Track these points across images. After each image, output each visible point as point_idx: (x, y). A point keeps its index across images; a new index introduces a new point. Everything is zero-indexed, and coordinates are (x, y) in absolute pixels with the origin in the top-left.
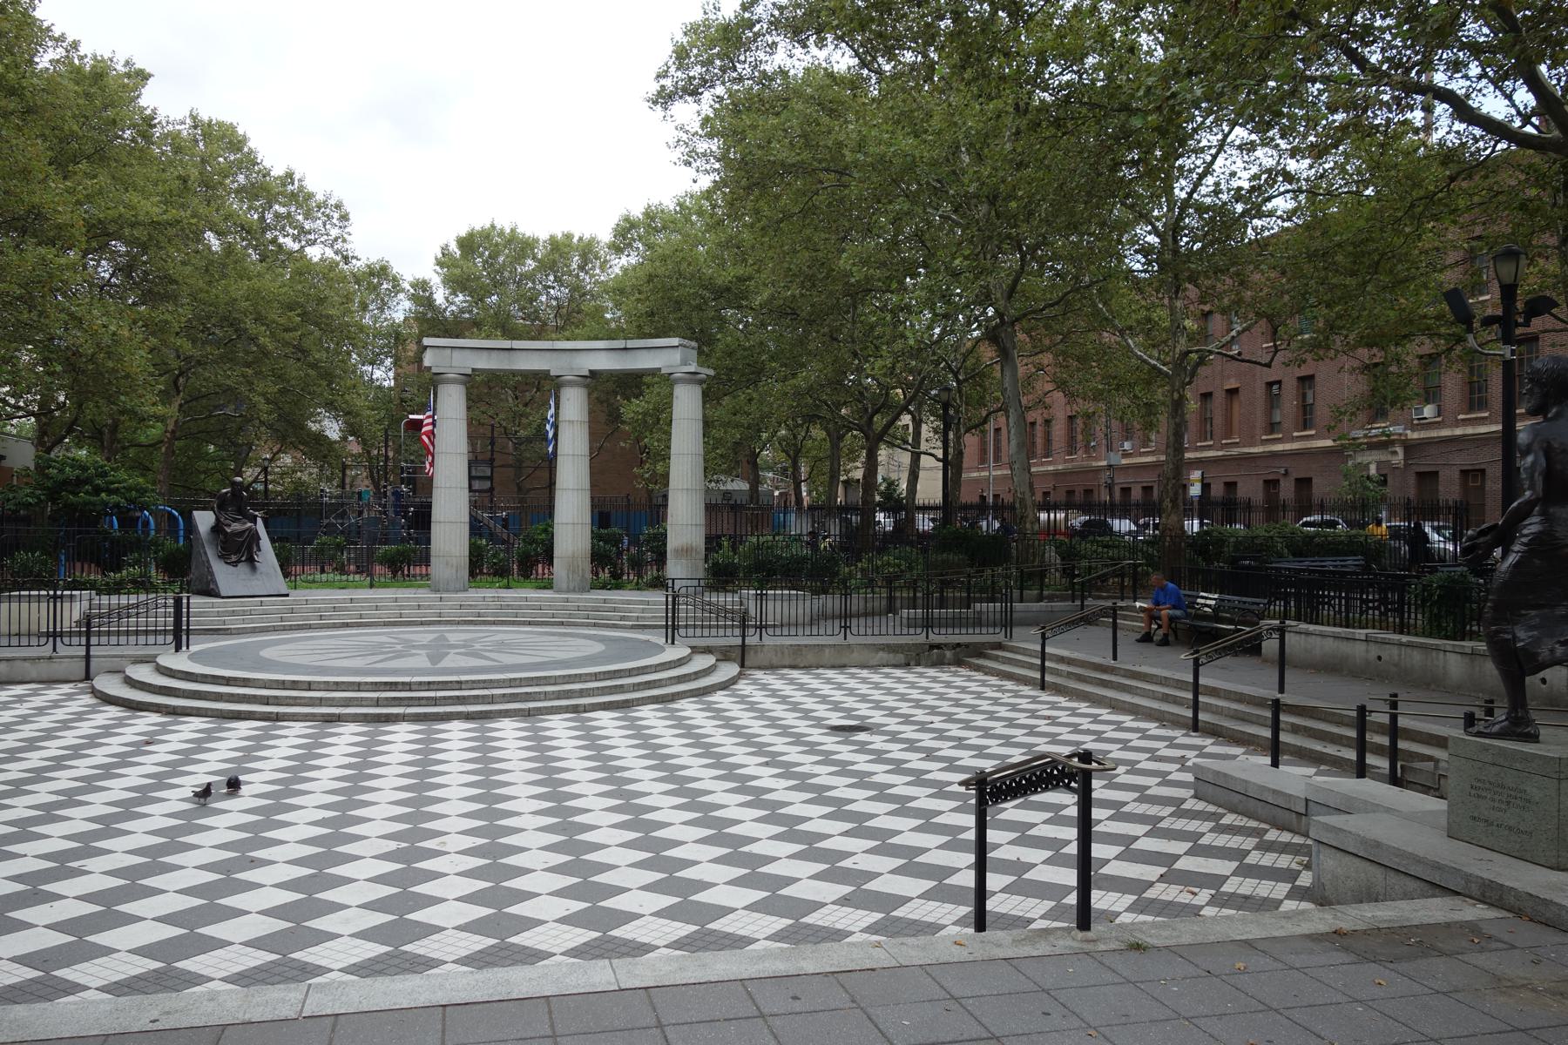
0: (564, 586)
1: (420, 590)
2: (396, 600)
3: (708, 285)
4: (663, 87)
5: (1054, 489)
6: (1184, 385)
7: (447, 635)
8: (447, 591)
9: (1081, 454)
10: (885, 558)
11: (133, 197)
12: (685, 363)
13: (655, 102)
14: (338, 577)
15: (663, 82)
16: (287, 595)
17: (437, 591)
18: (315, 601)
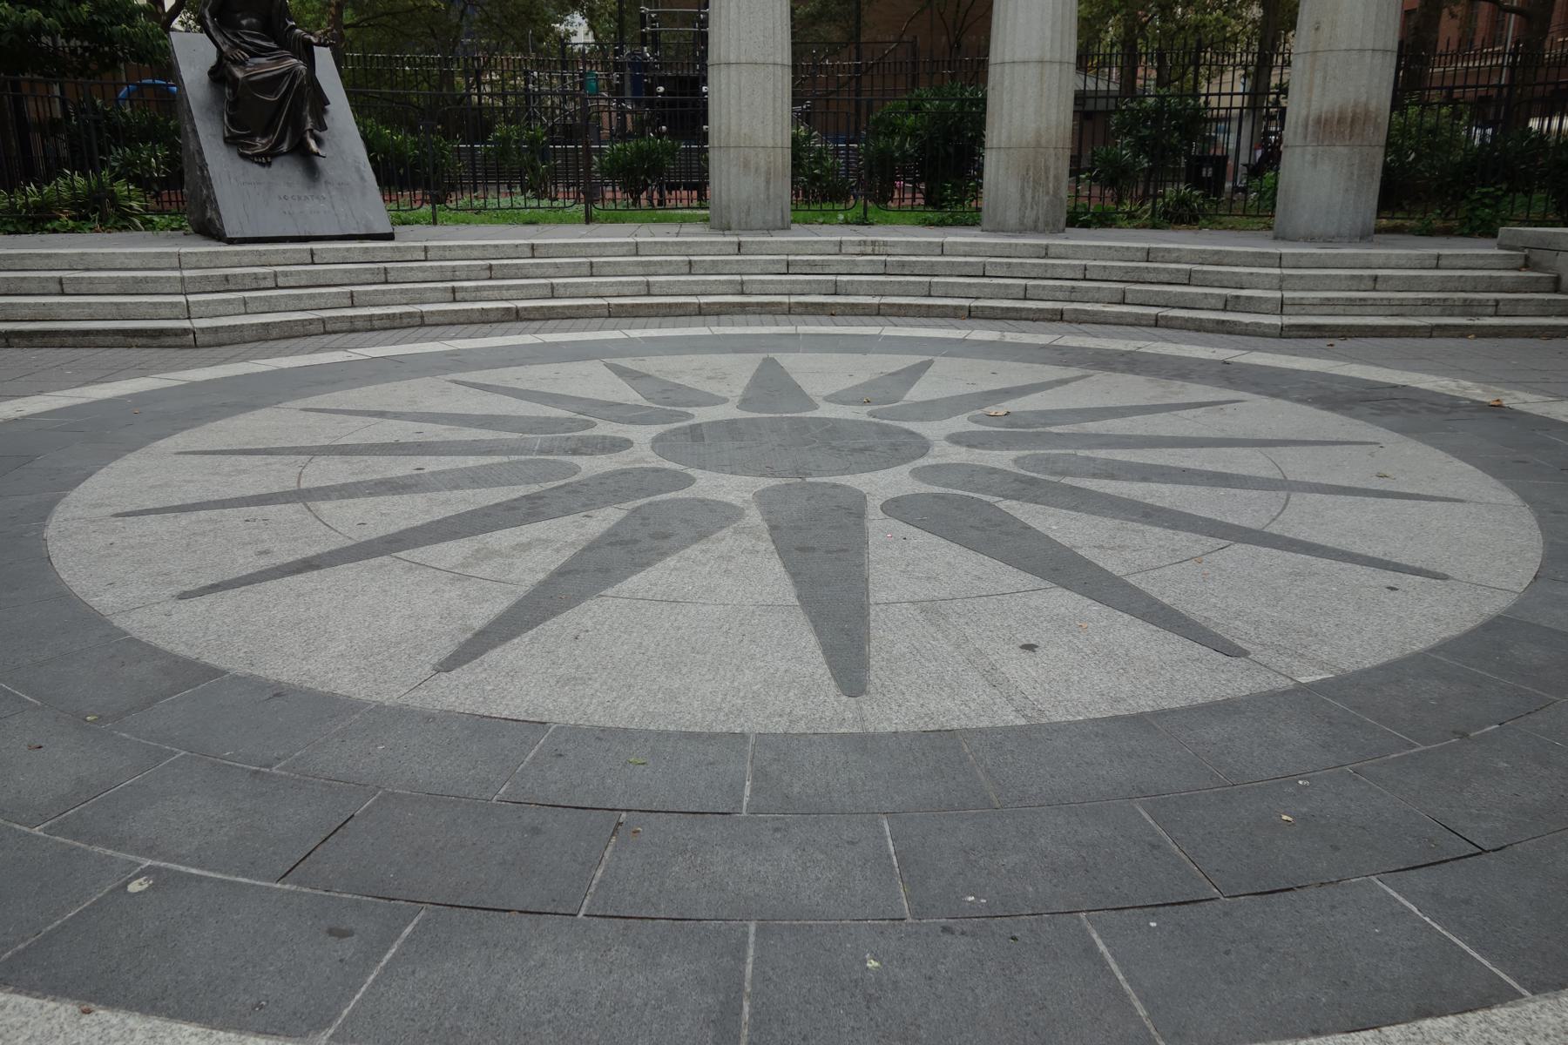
0: (1012, 217)
1: (687, 228)
2: (636, 249)
7: (787, 360)
8: (749, 229)
14: (534, 203)
16: (389, 237)
17: (725, 228)
18: (446, 253)
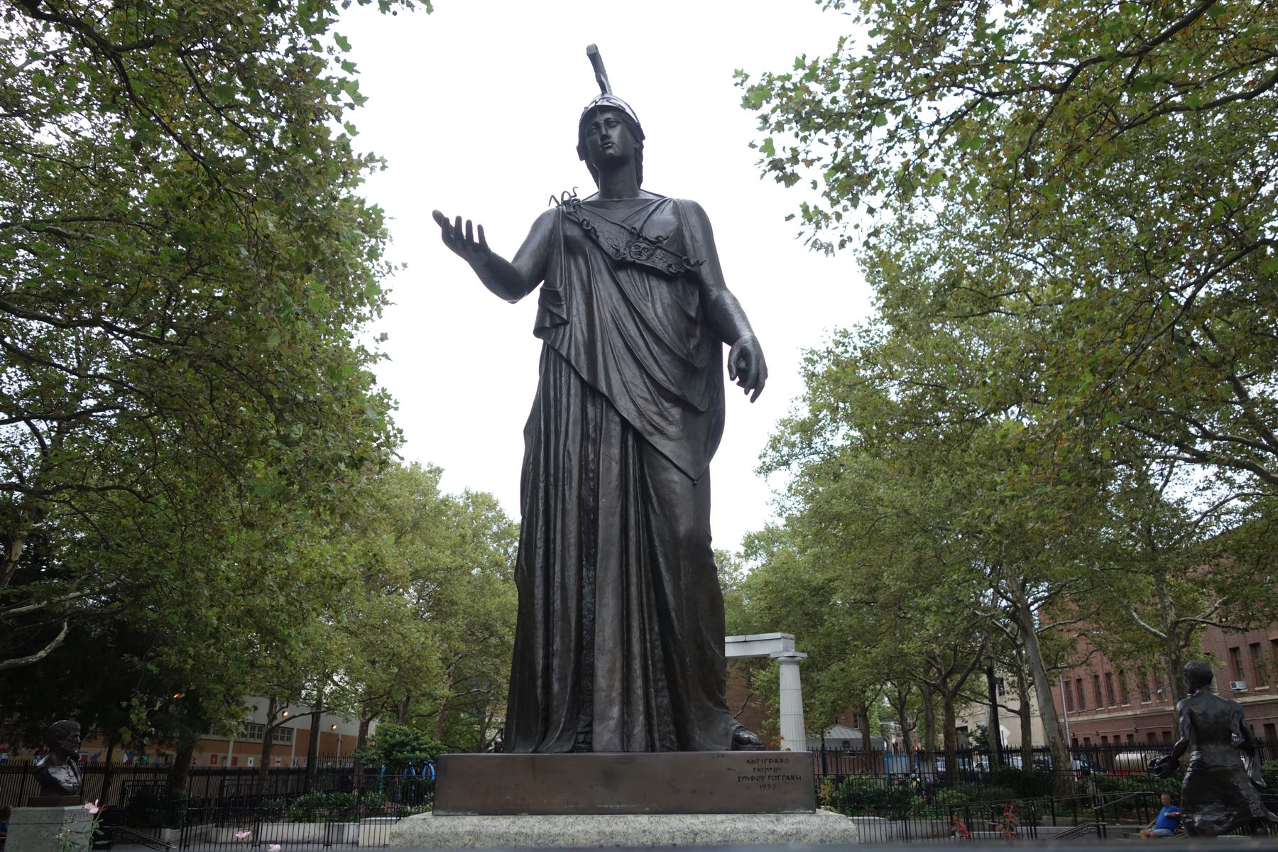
3: (806, 586)
4: (764, 462)
5: (1137, 731)
6: (1179, 648)
9: (1153, 700)
10: (950, 792)
11: (433, 552)
12: (786, 650)
13: (760, 473)
15: (763, 460)
